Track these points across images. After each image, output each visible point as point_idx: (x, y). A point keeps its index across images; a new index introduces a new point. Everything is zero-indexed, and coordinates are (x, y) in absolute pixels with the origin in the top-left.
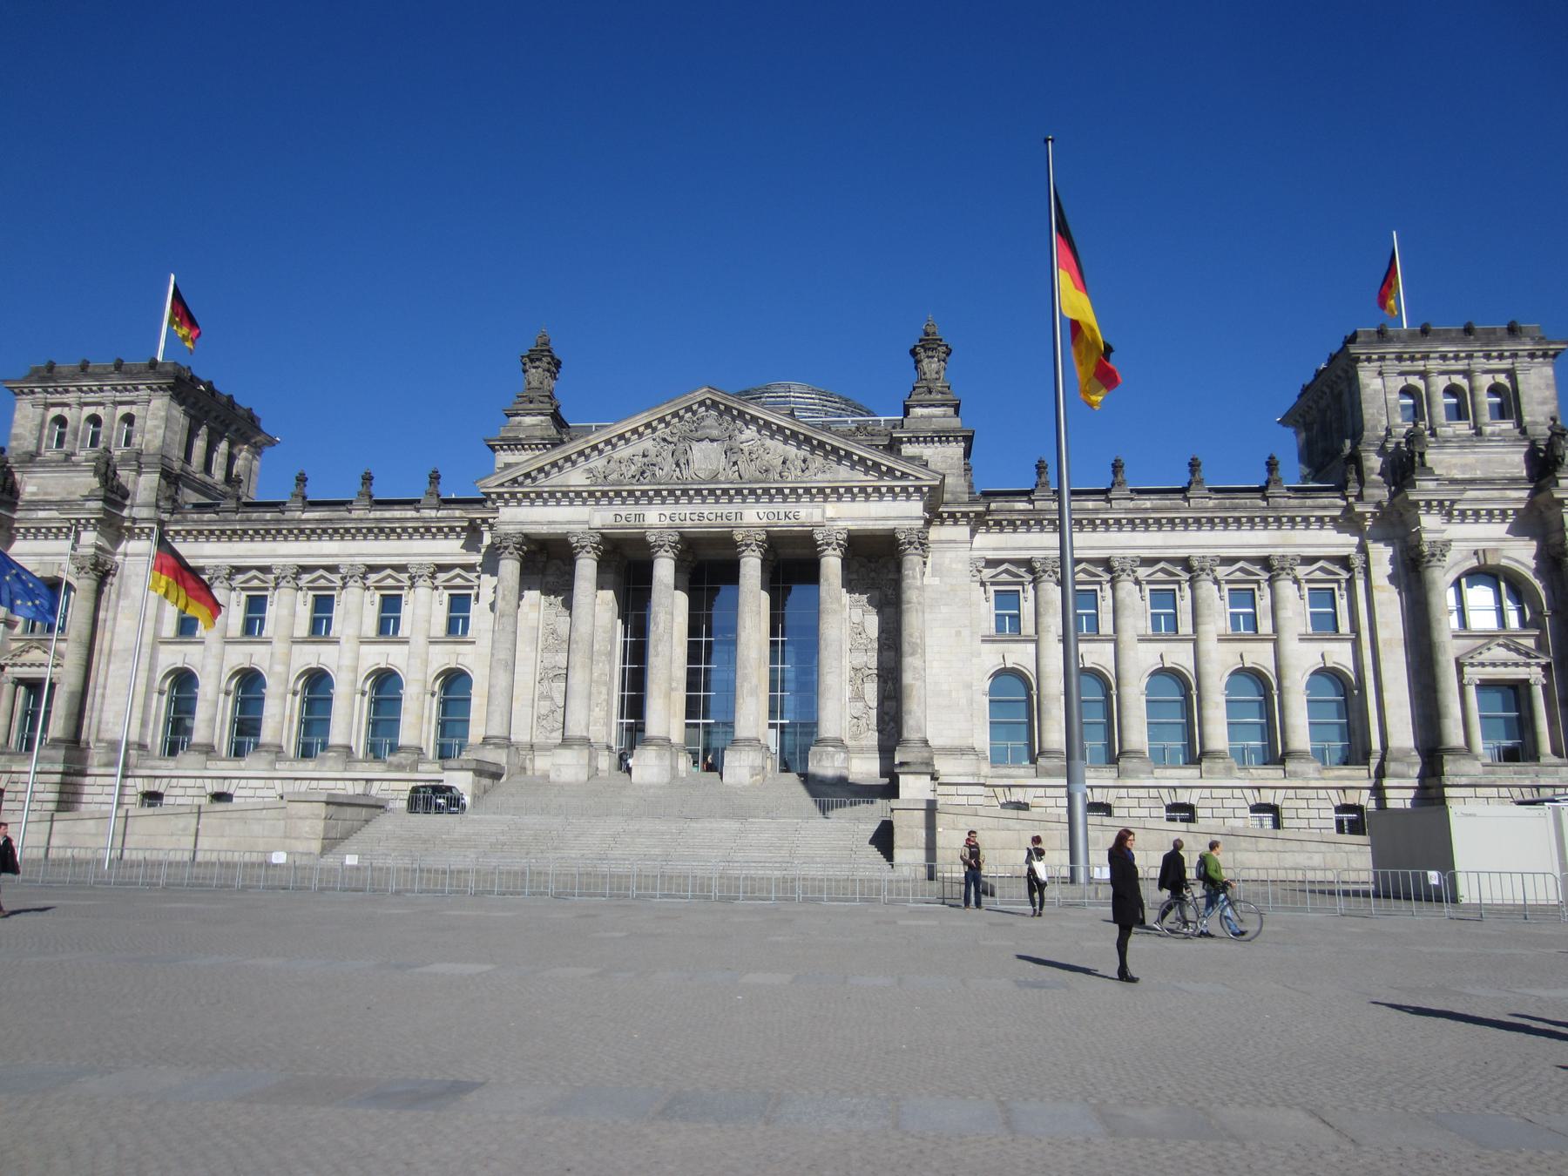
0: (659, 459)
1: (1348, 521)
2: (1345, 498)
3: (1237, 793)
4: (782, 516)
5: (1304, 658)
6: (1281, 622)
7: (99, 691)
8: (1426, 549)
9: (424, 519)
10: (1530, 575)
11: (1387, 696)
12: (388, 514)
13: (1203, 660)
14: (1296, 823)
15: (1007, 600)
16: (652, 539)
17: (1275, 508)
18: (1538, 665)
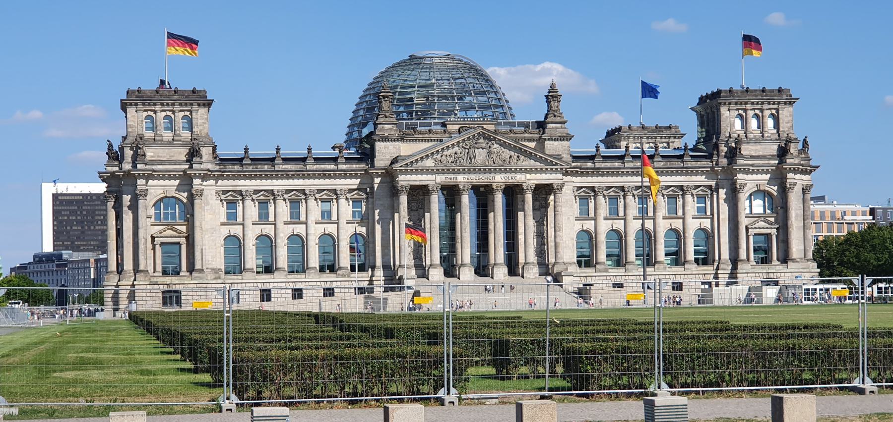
0: (462, 155)
1: (711, 173)
2: (712, 162)
3: (667, 276)
4: (510, 178)
5: (693, 225)
6: (686, 211)
7: (204, 247)
8: (738, 186)
9: (344, 171)
10: (775, 194)
11: (721, 240)
12: (323, 167)
13: (657, 226)
14: (688, 287)
15: (584, 200)
16: (461, 187)
17: (686, 168)
18: (774, 228)
